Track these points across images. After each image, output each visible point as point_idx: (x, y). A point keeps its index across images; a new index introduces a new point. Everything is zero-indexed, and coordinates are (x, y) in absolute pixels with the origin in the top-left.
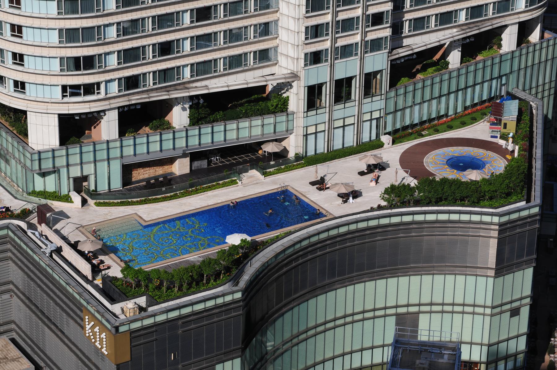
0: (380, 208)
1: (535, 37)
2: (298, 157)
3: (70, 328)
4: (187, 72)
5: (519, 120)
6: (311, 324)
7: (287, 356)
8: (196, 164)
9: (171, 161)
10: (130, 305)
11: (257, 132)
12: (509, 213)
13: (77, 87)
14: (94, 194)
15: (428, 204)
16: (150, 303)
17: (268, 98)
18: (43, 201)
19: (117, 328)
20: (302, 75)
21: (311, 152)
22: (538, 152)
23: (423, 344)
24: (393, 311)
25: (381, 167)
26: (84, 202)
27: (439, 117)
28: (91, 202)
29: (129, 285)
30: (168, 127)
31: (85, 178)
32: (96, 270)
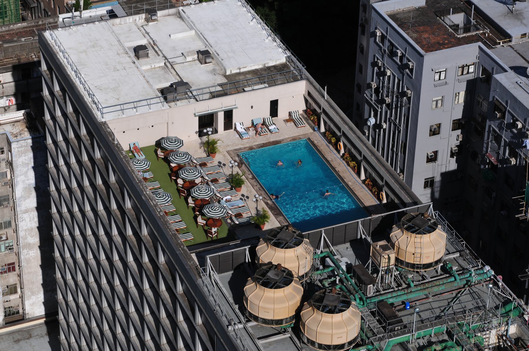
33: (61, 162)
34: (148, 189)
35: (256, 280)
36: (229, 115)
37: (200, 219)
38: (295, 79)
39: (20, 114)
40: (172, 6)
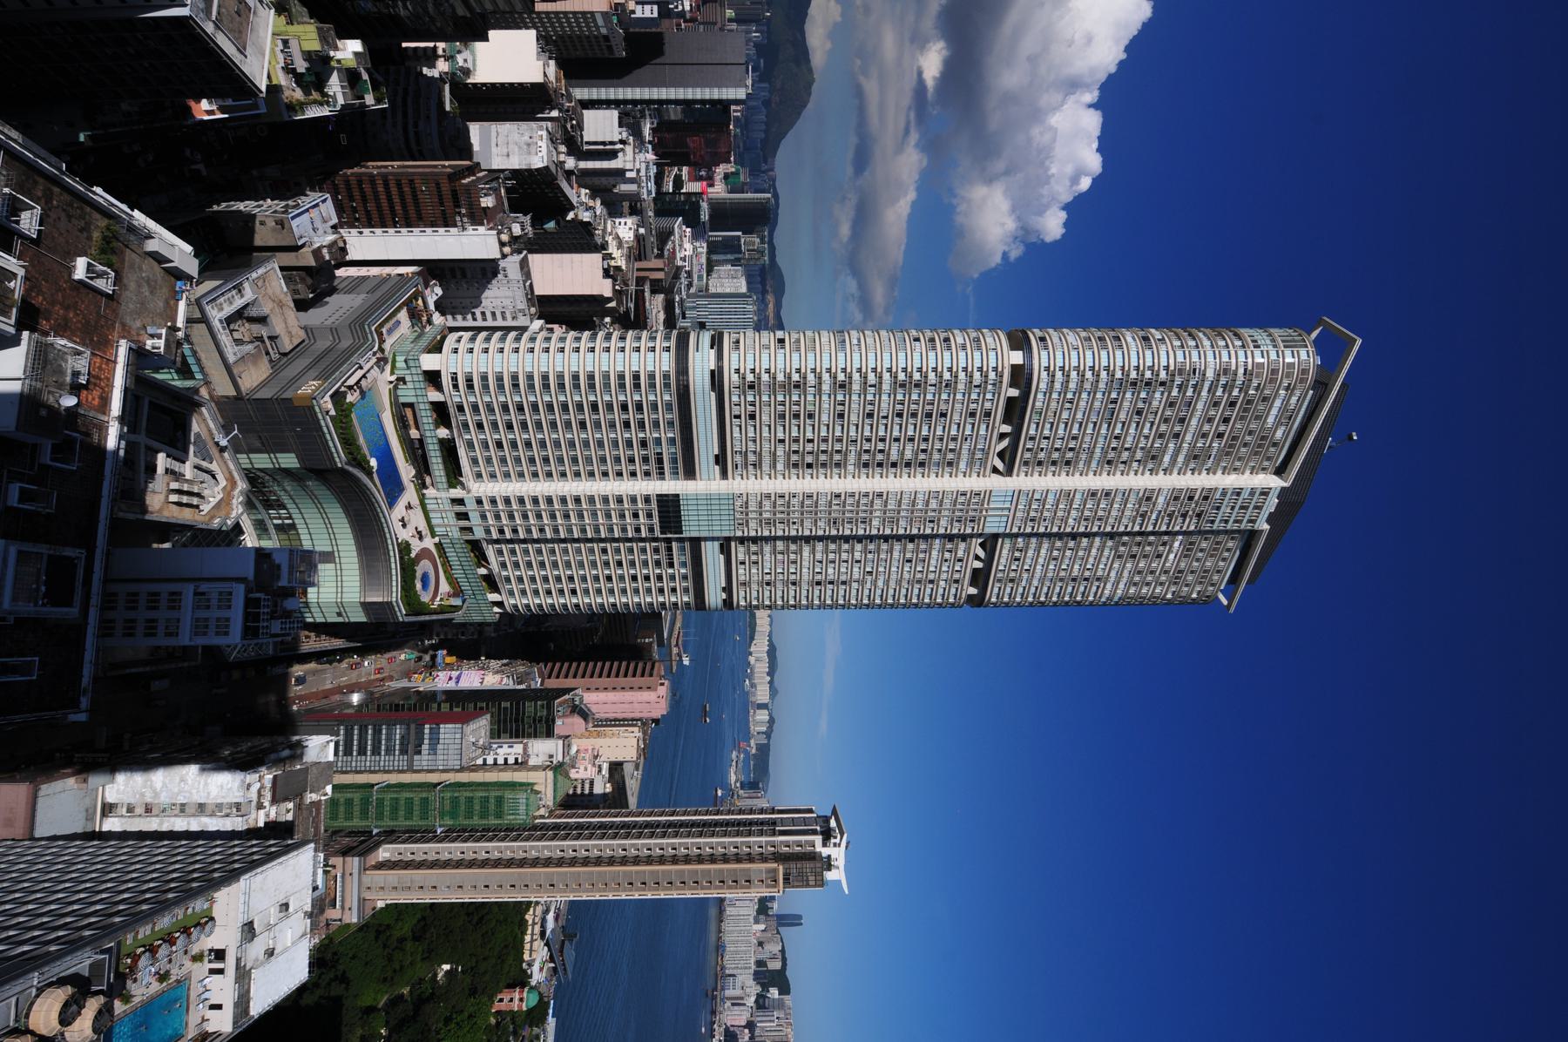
0: (397, 539)
1: (496, 609)
2: (424, 495)
5: (451, 606)
6: (325, 506)
7: (303, 493)
8: (417, 442)
9: (417, 428)
10: (330, 406)
11: (437, 473)
12: (398, 606)
13: (456, 380)
14: (396, 388)
15: (401, 564)
16: (331, 417)
17: (456, 478)
18: (390, 361)
20: (470, 495)
21: (427, 501)
22: (434, 617)
23: (316, 566)
24: (335, 549)
25: (421, 538)
26: (391, 382)
27: (450, 566)
28: (391, 386)
29: (342, 406)
30: (437, 427)
31: (405, 383)
32: (350, 388)
33: (218, 850)
34: (179, 912)
35: (73, 996)
36: (220, 971)
37: (142, 949)
38: (234, 1023)
39: (261, 824)
40: (311, 930)
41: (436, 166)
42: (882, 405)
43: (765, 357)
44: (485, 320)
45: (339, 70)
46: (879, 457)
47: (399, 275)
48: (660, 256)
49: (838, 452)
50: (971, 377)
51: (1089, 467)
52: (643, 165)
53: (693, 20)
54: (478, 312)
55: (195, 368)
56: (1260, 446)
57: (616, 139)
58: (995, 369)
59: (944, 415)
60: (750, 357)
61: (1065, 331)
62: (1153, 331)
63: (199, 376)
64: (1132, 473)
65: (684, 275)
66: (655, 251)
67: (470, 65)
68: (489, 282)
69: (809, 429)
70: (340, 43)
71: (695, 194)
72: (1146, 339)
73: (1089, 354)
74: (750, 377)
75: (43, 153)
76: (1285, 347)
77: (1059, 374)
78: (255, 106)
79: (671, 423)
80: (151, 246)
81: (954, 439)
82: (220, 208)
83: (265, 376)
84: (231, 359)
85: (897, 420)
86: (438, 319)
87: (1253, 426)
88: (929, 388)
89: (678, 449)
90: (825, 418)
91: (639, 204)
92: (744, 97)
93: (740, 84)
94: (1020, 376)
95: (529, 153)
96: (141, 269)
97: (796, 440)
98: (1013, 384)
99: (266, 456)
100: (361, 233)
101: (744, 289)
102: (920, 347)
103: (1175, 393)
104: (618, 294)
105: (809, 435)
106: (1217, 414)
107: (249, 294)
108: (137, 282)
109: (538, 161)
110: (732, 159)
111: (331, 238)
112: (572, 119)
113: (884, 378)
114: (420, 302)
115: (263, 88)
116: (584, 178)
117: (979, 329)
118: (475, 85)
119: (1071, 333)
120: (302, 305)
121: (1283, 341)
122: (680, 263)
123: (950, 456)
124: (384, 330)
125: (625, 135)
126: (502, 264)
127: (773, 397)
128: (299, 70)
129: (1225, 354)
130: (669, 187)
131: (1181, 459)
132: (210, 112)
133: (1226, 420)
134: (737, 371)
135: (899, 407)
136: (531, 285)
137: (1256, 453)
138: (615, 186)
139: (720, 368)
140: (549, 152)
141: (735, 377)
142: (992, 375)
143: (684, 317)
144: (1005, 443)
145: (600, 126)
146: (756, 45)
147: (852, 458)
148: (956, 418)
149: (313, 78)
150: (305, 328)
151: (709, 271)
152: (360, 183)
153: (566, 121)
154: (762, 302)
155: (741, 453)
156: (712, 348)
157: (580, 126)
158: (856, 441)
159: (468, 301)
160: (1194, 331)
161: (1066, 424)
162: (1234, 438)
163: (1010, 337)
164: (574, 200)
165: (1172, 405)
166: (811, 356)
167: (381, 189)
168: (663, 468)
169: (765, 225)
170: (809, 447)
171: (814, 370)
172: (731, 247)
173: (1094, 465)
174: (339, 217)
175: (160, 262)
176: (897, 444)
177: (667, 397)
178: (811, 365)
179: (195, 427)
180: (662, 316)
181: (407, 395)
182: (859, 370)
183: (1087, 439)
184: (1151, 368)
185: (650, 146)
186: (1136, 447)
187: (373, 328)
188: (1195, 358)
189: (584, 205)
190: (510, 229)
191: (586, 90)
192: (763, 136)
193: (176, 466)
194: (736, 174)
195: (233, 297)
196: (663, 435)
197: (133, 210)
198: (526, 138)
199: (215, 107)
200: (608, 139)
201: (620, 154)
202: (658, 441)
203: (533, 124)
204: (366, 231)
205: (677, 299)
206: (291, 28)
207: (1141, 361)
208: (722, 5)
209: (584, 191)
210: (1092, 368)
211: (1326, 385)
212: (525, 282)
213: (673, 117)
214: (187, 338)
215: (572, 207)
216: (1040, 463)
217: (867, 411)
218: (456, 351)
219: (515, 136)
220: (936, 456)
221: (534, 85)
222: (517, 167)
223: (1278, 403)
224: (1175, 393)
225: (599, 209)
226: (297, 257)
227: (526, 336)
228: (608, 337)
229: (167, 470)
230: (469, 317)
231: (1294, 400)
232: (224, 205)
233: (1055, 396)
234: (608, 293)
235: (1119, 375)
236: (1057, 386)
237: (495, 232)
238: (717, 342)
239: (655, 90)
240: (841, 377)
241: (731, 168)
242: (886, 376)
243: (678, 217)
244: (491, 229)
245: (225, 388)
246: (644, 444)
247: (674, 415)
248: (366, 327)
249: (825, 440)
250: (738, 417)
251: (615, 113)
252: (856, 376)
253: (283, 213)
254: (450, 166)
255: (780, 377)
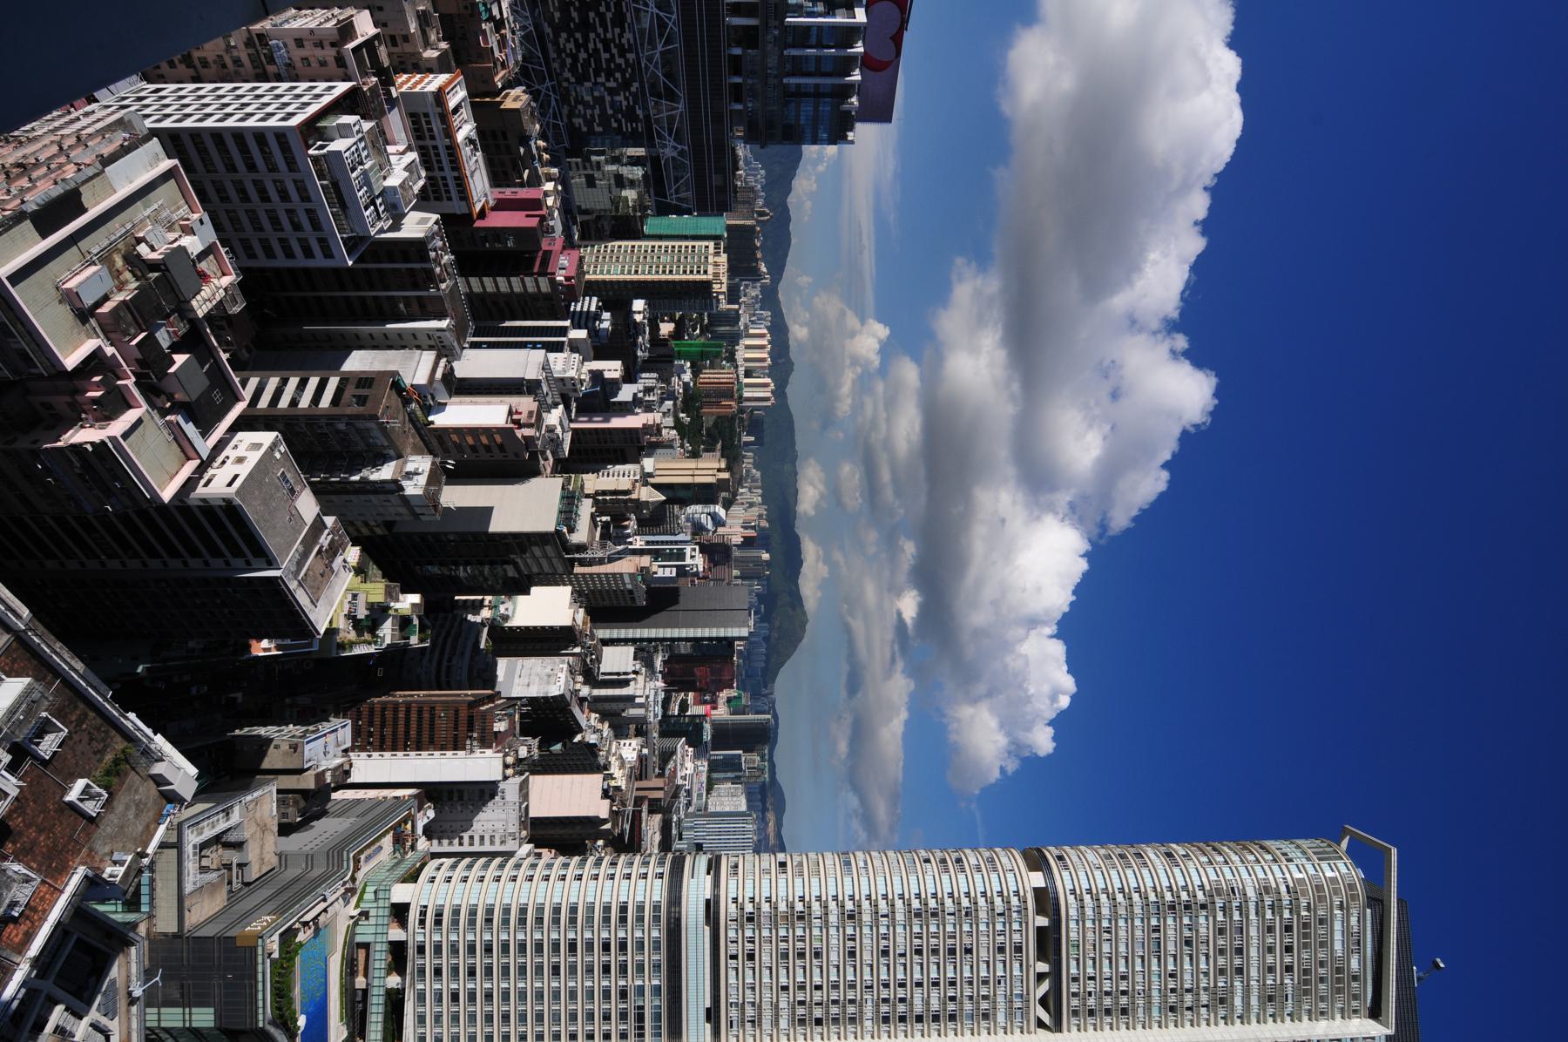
3: (271, 906)
4: (421, 987)
8: (360, 993)
9: (366, 975)
10: (276, 946)
13: (425, 915)
14: (356, 924)
16: (273, 962)
18: (359, 892)
19: (261, 937)
26: (352, 917)
28: (351, 922)
29: (290, 946)
30: (389, 973)
31: (367, 918)
32: (306, 924)
41: (459, 695)
42: (898, 939)
43: (765, 883)
44: (471, 844)
45: (394, 617)
46: (901, 1008)
47: (396, 798)
48: (661, 775)
49: (852, 1002)
50: (992, 903)
51: (1150, 1016)
52: (653, 692)
53: (705, 578)
54: (466, 836)
55: (145, 899)
56: (1339, 980)
57: (630, 670)
58: (1017, 893)
59: (969, 951)
60: (749, 884)
61: (1082, 847)
62: (1174, 846)
63: (145, 908)
64: (1204, 1023)
65: (683, 793)
66: (657, 770)
67: (510, 613)
68: (484, 805)
69: (816, 971)
70: (401, 597)
71: (699, 716)
72: (1169, 855)
73: (1113, 873)
74: (749, 908)
75: (96, 681)
76: (1319, 859)
77: (1087, 898)
78: (310, 645)
79: (657, 967)
80: (158, 769)
81: (986, 982)
82: (242, 733)
83: (217, 909)
84: (189, 887)
85: (916, 958)
86: (423, 844)
87: (1321, 955)
88: (948, 917)
89: (663, 1002)
90: (833, 957)
91: (644, 727)
92: (747, 635)
93: (744, 624)
94: (1046, 900)
95: (548, 683)
96: (136, 791)
97: (802, 988)
98: (1040, 911)
99: (180, 1010)
100: (370, 756)
101: (743, 808)
102: (932, 869)
103: (1220, 917)
104: (614, 815)
105: (817, 980)
106: (1276, 939)
107: (236, 817)
108: (127, 804)
109: (555, 690)
110: (735, 685)
111: (339, 761)
112: (592, 654)
113: (897, 906)
114: (409, 826)
115: (322, 631)
116: (595, 704)
117: (991, 848)
118: (510, 628)
119: (1088, 851)
120: (285, 830)
121: (1315, 853)
122: (680, 782)
123: (984, 1005)
124: (362, 857)
125: (638, 667)
126: (502, 786)
127: (774, 931)
128: (358, 617)
129: (1258, 868)
130: (675, 710)
131: (1254, 1001)
132: (265, 650)
133: (1289, 949)
134: (735, 900)
135: (917, 942)
136: (527, 807)
137: (1339, 991)
138: (624, 711)
139: (716, 897)
140: (567, 682)
141: (732, 907)
142: (1015, 901)
143: (681, 838)
144: (1045, 986)
145: (617, 659)
146: (758, 595)
147: (868, 1010)
148: (983, 953)
149: (370, 623)
150: (279, 855)
151: (709, 790)
152: (384, 709)
153: (586, 656)
154: (763, 820)
155: (737, 1004)
156: (708, 873)
157: (599, 660)
158: (871, 987)
159: (459, 824)
160: (1217, 845)
161: (1110, 959)
162: (1306, 972)
163: (1026, 856)
164: (583, 723)
165: (1221, 931)
166: (815, 881)
167: (401, 715)
168: (642, 1028)
169: (765, 743)
170: (817, 997)
171: (819, 898)
172: (732, 765)
173: (1155, 1013)
174: (354, 740)
175: (158, 785)
176: (919, 990)
177: (655, 934)
178: (815, 892)
179: (114, 972)
180: (657, 838)
181: (365, 933)
182: (869, 897)
183: (1139, 978)
184: (1185, 888)
185: (660, 676)
186: (1198, 987)
187: (352, 855)
188: (1229, 876)
189: (591, 728)
190: (517, 752)
191: (608, 631)
192: (763, 665)
193: (69, 1022)
194: (739, 697)
195: (218, 820)
196: (647, 982)
197: (155, 734)
198: (548, 670)
199: (272, 646)
200: (622, 670)
201: (632, 683)
202: (640, 991)
203: (557, 659)
204: (376, 754)
205: (675, 819)
206: (363, 586)
207: (1172, 881)
208: (730, 567)
209: (594, 715)
210: (1122, 890)
211: (1382, 902)
212: (521, 804)
213: (683, 652)
214: (151, 868)
215: (580, 730)
216: (1091, 1013)
217: (881, 948)
218: (432, 880)
219: (539, 669)
220: (968, 1006)
221: (562, 627)
222: (535, 695)
223: (1338, 926)
224: (1220, 917)
225: (606, 729)
226: (298, 779)
227: (512, 862)
228: (598, 863)
229: (57, 1027)
230: (456, 841)
231: (1354, 921)
232: (246, 729)
233: (1089, 924)
234: (604, 814)
235: (1152, 897)
236: (1089, 912)
237: (501, 755)
238: (714, 867)
239: (669, 630)
240: (849, 906)
241: (733, 693)
242: (899, 904)
243: (681, 737)
244: (498, 752)
245: (166, 923)
246: (623, 994)
247: (662, 957)
248: (345, 853)
249: (836, 987)
250: (734, 957)
251: (631, 650)
252: (866, 904)
253: (300, 737)
254: (472, 695)
255: (782, 907)
